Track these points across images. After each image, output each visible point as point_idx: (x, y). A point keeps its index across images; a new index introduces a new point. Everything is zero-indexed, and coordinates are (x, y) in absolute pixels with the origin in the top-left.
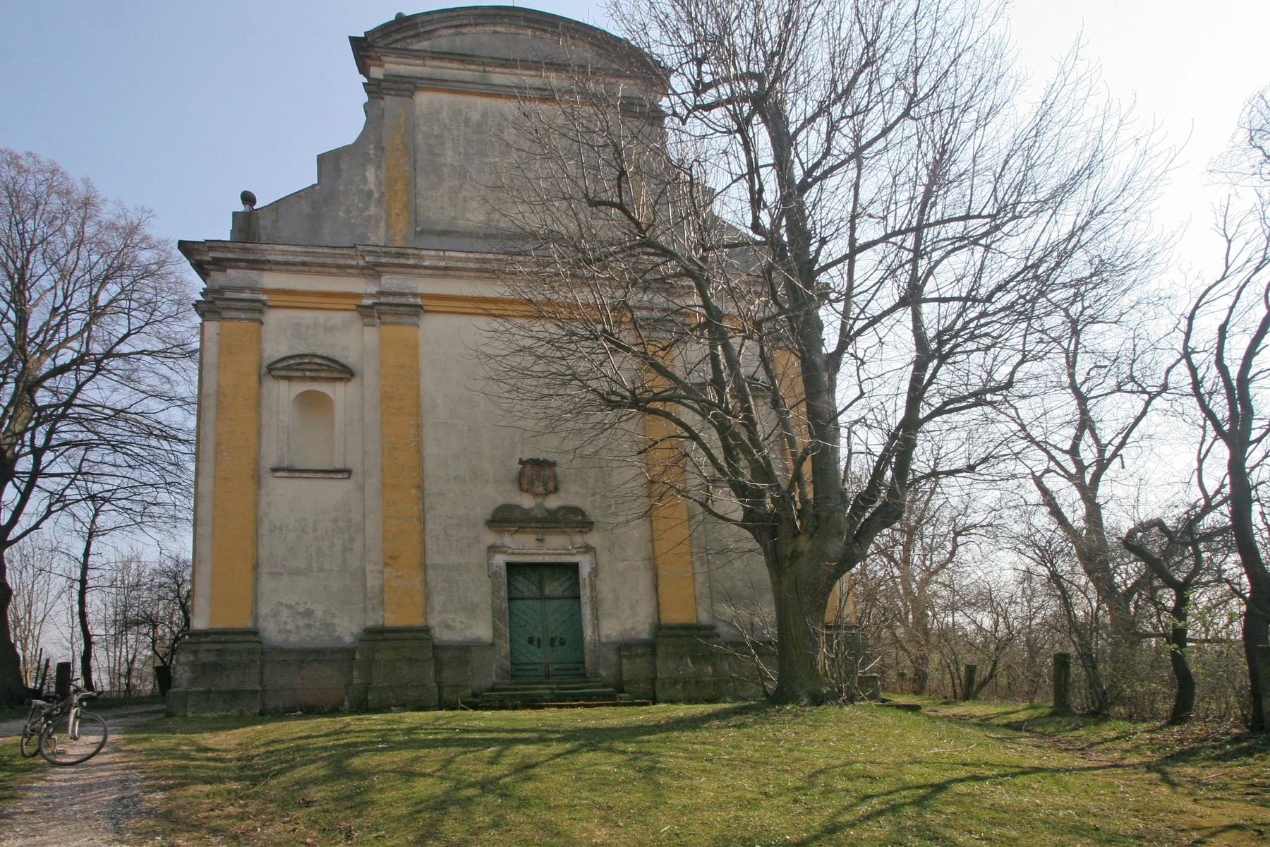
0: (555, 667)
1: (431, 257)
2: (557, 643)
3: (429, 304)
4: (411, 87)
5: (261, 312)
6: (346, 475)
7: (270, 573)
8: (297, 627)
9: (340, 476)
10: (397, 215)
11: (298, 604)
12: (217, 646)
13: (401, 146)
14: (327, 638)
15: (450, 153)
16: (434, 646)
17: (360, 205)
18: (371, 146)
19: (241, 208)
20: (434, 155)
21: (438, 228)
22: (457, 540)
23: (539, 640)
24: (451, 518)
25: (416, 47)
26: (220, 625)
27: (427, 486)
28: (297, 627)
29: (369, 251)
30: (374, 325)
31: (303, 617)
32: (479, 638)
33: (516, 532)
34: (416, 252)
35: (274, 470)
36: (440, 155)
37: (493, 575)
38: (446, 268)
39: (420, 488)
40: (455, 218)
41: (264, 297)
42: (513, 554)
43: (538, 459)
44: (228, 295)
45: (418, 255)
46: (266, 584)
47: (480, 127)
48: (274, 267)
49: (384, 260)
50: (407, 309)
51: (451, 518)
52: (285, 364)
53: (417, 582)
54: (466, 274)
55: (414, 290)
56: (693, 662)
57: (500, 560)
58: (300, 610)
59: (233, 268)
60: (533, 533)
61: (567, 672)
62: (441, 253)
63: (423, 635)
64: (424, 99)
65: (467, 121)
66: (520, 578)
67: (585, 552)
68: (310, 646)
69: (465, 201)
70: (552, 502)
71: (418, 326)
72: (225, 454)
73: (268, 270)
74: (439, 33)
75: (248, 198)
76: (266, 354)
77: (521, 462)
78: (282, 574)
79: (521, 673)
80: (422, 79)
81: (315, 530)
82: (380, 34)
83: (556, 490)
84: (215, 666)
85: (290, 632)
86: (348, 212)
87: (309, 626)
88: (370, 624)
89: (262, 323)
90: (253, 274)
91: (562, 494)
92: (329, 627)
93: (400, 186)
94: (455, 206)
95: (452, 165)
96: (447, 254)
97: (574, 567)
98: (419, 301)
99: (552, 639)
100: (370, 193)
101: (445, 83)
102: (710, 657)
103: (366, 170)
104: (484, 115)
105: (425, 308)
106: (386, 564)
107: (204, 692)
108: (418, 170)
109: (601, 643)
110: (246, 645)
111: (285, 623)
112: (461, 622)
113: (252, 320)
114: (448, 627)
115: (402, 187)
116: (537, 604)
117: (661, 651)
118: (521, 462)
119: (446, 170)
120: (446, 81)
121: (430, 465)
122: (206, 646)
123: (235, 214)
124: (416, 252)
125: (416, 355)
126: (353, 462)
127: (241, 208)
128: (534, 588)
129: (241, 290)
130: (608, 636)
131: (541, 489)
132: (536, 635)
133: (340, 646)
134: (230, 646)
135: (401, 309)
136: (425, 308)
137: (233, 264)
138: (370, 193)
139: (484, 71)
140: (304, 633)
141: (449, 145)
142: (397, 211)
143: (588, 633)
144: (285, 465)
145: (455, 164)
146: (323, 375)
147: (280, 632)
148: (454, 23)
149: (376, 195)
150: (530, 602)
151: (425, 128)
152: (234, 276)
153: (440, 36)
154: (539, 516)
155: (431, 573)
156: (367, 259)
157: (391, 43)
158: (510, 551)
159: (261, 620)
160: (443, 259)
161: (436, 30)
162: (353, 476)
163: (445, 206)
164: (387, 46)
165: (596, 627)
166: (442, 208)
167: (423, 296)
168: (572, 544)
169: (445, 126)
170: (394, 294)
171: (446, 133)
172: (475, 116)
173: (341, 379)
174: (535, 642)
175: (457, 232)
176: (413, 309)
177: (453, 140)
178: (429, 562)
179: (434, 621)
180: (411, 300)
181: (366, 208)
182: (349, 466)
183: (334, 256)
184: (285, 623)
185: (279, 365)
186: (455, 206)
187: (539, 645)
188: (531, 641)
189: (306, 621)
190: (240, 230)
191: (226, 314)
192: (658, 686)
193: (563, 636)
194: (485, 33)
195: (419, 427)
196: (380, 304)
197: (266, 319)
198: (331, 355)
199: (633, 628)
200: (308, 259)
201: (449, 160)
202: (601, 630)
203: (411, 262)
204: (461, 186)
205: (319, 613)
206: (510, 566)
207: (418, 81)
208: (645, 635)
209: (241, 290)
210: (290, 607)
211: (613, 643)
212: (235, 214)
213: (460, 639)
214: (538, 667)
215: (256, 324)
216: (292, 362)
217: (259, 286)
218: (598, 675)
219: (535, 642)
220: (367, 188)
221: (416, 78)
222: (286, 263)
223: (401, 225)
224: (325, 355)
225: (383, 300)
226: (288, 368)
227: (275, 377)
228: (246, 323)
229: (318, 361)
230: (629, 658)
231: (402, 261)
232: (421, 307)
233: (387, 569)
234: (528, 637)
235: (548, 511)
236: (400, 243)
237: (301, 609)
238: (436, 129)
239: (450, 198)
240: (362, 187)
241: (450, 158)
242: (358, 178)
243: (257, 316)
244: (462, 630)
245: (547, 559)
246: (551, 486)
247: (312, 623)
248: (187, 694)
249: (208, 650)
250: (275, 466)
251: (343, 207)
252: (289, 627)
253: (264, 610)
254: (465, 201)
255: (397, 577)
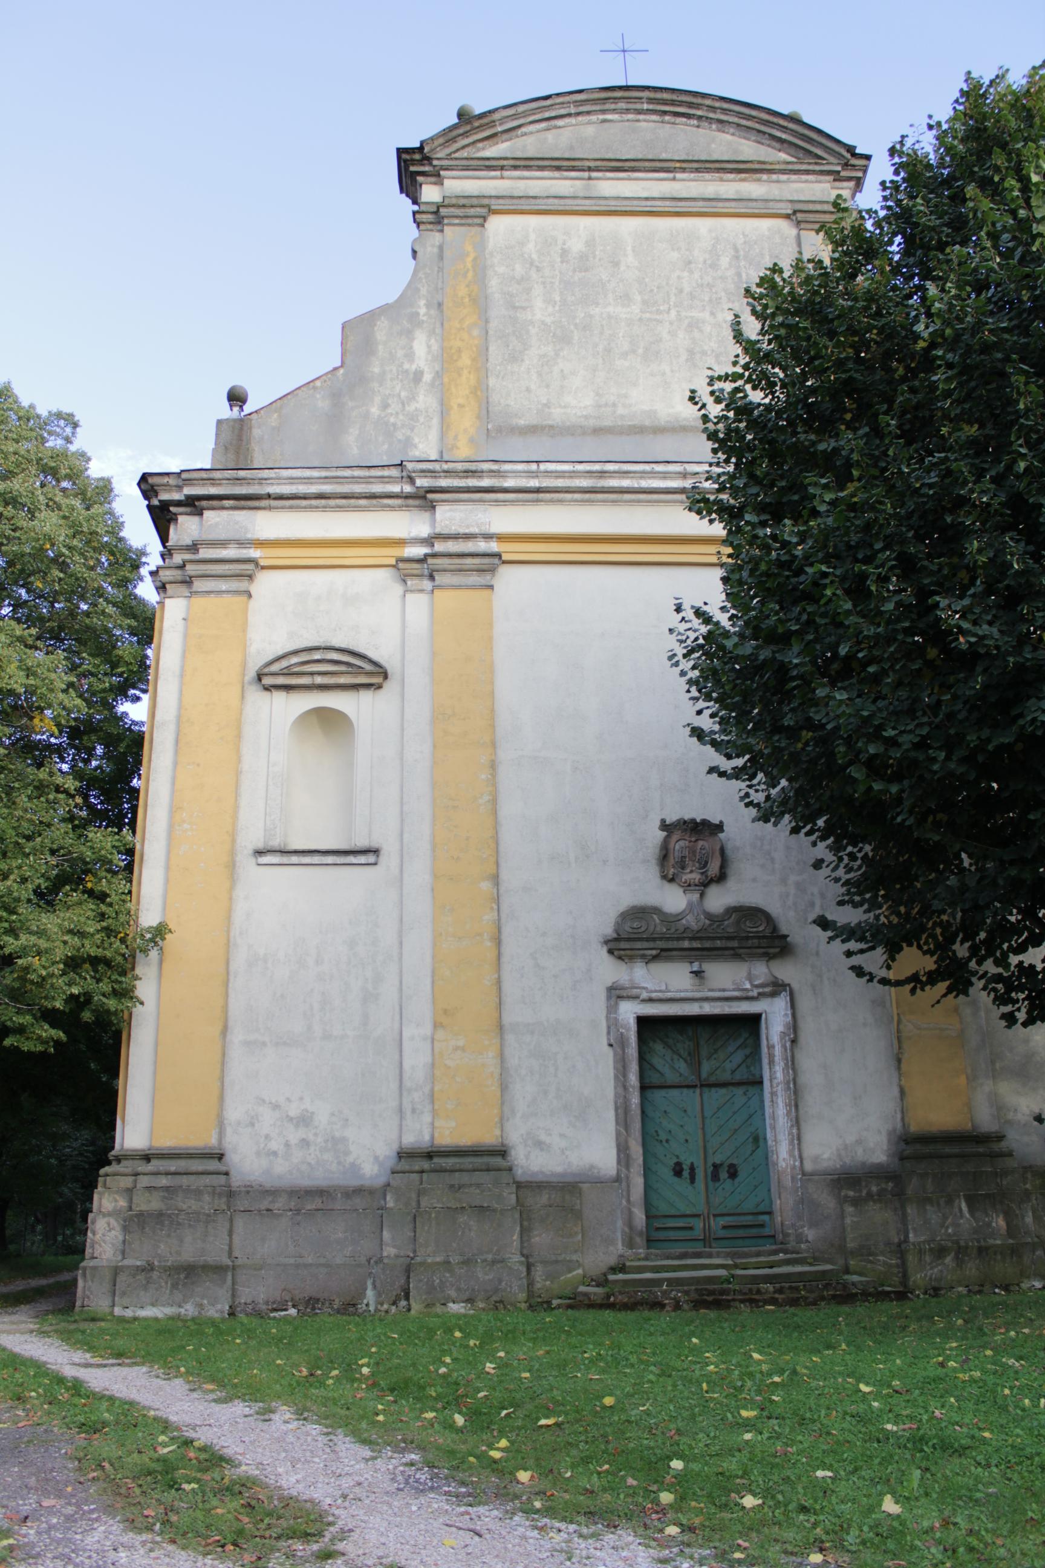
0: (722, 1221)
1: (516, 474)
2: (723, 1175)
3: (509, 550)
4: (483, 211)
5: (250, 577)
6: (371, 858)
7: (247, 1043)
8: (287, 1145)
9: (362, 859)
10: (460, 406)
11: (289, 1100)
12: (164, 1181)
13: (467, 300)
14: (334, 1167)
15: (538, 303)
16: (519, 1185)
17: (403, 394)
18: (422, 302)
19: (225, 411)
20: (515, 308)
21: (522, 422)
22: (555, 976)
23: (692, 1169)
24: (544, 934)
25: (487, 153)
26: (166, 1141)
27: (504, 875)
28: (287, 1145)
29: (423, 471)
30: (421, 591)
31: (297, 1126)
32: (592, 1167)
33: (655, 958)
34: (495, 467)
35: (259, 853)
36: (524, 308)
37: (617, 1043)
38: (538, 490)
39: (496, 879)
40: (547, 405)
41: (254, 553)
42: (651, 1000)
43: (693, 821)
44: (204, 553)
45: (499, 471)
46: (239, 1063)
47: (584, 262)
48: (273, 503)
49: (444, 483)
50: (477, 561)
51: (544, 934)
52: (284, 663)
53: (490, 1058)
54: (569, 496)
55: (485, 529)
56: (971, 1211)
57: (629, 1012)
58: (292, 1114)
59: (213, 508)
60: (682, 959)
61: (741, 1233)
62: (534, 467)
63: (497, 1161)
64: (498, 226)
65: (564, 253)
66: (659, 1047)
67: (773, 994)
68: (306, 1183)
69: (564, 377)
70: (718, 900)
71: (491, 587)
72: (186, 826)
73: (264, 508)
74: (524, 130)
75: (236, 398)
76: (253, 649)
77: (664, 826)
78: (264, 1044)
79: (662, 1235)
80: (498, 197)
81: (318, 962)
82: (441, 140)
83: (721, 878)
84: (159, 1217)
85: (275, 1154)
86: (385, 406)
87: (305, 1143)
88: (410, 1140)
89: (250, 596)
90: (241, 516)
91: (731, 883)
92: (336, 1143)
93: (465, 360)
94: (548, 386)
95: (543, 322)
96: (543, 467)
97: (754, 1020)
98: (494, 546)
99: (716, 1167)
100: (418, 376)
101: (533, 201)
102: (999, 1200)
103: (413, 339)
104: (590, 243)
105: (505, 557)
106: (436, 1025)
107: (143, 1270)
108: (491, 332)
109: (804, 1174)
110: (207, 1180)
111: (267, 1137)
112: (562, 1135)
113: (237, 592)
114: (540, 1144)
115: (468, 362)
116: (691, 1098)
117: (913, 1186)
118: (664, 826)
119: (533, 331)
120: (535, 198)
121: (509, 837)
122: (144, 1181)
123: (219, 422)
124: (495, 467)
125: (490, 639)
126: (384, 837)
127: (225, 411)
128: (682, 1066)
129: (223, 544)
130: (816, 1159)
131: (696, 877)
132: (686, 1160)
133: (355, 1183)
134: (185, 1181)
135: (469, 561)
136: (505, 557)
137: (215, 503)
138: (418, 376)
139: (590, 178)
140: (297, 1156)
141: (538, 290)
142: (461, 401)
143: (782, 1153)
144: (275, 843)
145: (548, 320)
146: (342, 680)
147: (258, 1154)
148: (547, 115)
149: (427, 377)
150: (675, 1093)
151: (501, 270)
152: (217, 522)
153: (525, 134)
154: (694, 926)
155: (510, 1038)
156: (419, 482)
157: (455, 152)
158: (645, 995)
159: (229, 1131)
160: (534, 475)
161: (519, 127)
162: (383, 859)
163: (533, 387)
164: (449, 157)
165: (798, 1139)
166: (528, 390)
167: (501, 538)
168: (750, 978)
169: (532, 264)
170: (455, 537)
171: (534, 274)
172: (576, 246)
173: (368, 686)
174: (686, 1173)
175: (551, 427)
176: (486, 560)
177: (544, 283)
178: (507, 1019)
179: (516, 1136)
180: (482, 546)
181: (412, 398)
182: (374, 845)
183: (367, 480)
184: (267, 1137)
185: (275, 668)
186: (548, 386)
187: (692, 1179)
188: (678, 1171)
189: (301, 1133)
190: (226, 448)
191: (198, 585)
192: (912, 1259)
193: (735, 1162)
194: (589, 123)
195: (493, 766)
196: (434, 555)
197: (254, 589)
198: (353, 646)
199: (859, 1142)
200: (327, 488)
201: (539, 316)
202: (804, 1146)
203: (486, 483)
204: (557, 355)
205: (322, 1118)
206: (643, 1022)
207: (493, 201)
208: (880, 1156)
209: (223, 544)
210: (276, 1107)
211: (825, 1173)
212: (219, 422)
213: (559, 1169)
214: (691, 1221)
215: (244, 598)
216: (295, 660)
217: (249, 536)
218: (800, 1238)
219: (686, 1173)
220: (414, 367)
221: (490, 197)
222: (357, 498)
223: (466, 423)
224: (343, 646)
225: (439, 547)
226: (287, 673)
227: (267, 689)
228: (227, 599)
229: (335, 656)
230: (856, 1202)
231: (472, 482)
232: (498, 555)
233: (440, 1034)
234: (672, 1162)
235: (709, 916)
236: (464, 451)
237: (294, 1111)
238: (519, 269)
239: (540, 374)
240: (406, 366)
241: (540, 311)
242: (400, 353)
243: (243, 585)
244: (563, 1151)
245: (708, 1009)
246: (714, 868)
247: (311, 1137)
248: (116, 1271)
249: (149, 1188)
250: (260, 845)
251: (377, 400)
252: (274, 1145)
253: (234, 1113)
254: (564, 377)
255: (457, 1048)
